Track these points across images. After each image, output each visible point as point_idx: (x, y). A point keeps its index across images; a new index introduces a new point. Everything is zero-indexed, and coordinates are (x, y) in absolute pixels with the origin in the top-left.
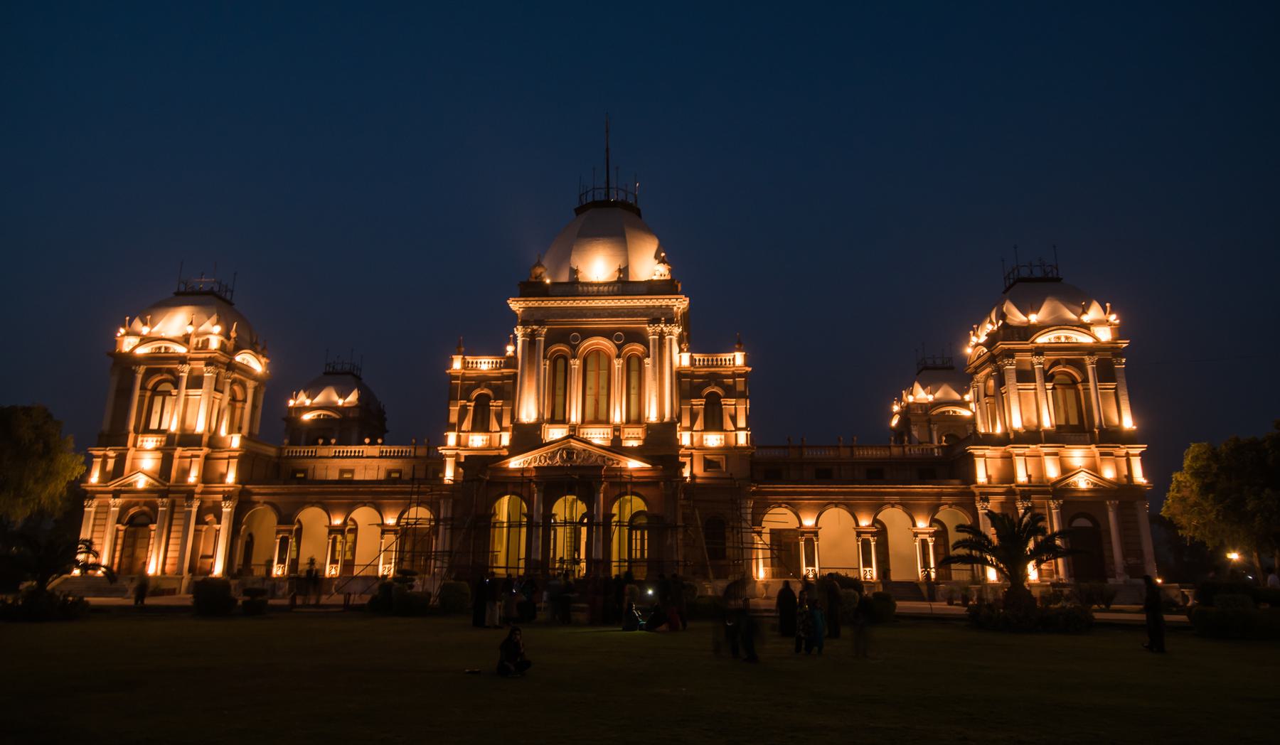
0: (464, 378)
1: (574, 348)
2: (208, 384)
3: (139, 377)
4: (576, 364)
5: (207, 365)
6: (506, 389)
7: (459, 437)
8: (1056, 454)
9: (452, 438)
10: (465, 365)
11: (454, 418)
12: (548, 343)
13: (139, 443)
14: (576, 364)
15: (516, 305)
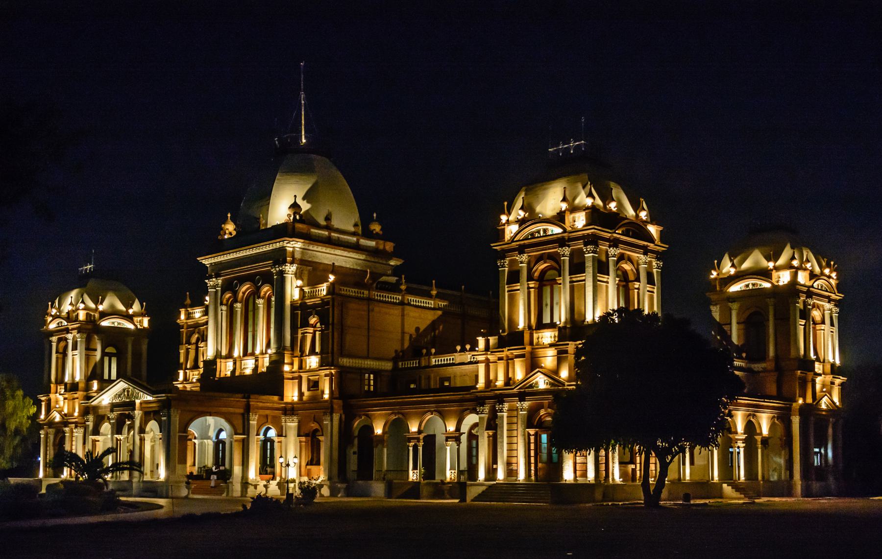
0: (189, 327)
1: (235, 294)
2: (81, 346)
3: (54, 345)
4: (238, 306)
5: (586, 245)
6: (199, 332)
7: (185, 374)
8: (522, 356)
9: (181, 373)
10: (189, 316)
11: (182, 360)
12: (223, 293)
13: (535, 341)
14: (238, 306)
15: (207, 261)
